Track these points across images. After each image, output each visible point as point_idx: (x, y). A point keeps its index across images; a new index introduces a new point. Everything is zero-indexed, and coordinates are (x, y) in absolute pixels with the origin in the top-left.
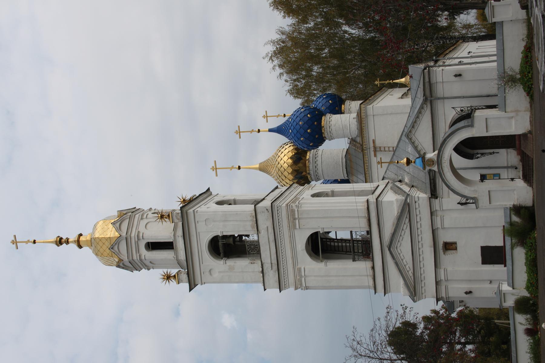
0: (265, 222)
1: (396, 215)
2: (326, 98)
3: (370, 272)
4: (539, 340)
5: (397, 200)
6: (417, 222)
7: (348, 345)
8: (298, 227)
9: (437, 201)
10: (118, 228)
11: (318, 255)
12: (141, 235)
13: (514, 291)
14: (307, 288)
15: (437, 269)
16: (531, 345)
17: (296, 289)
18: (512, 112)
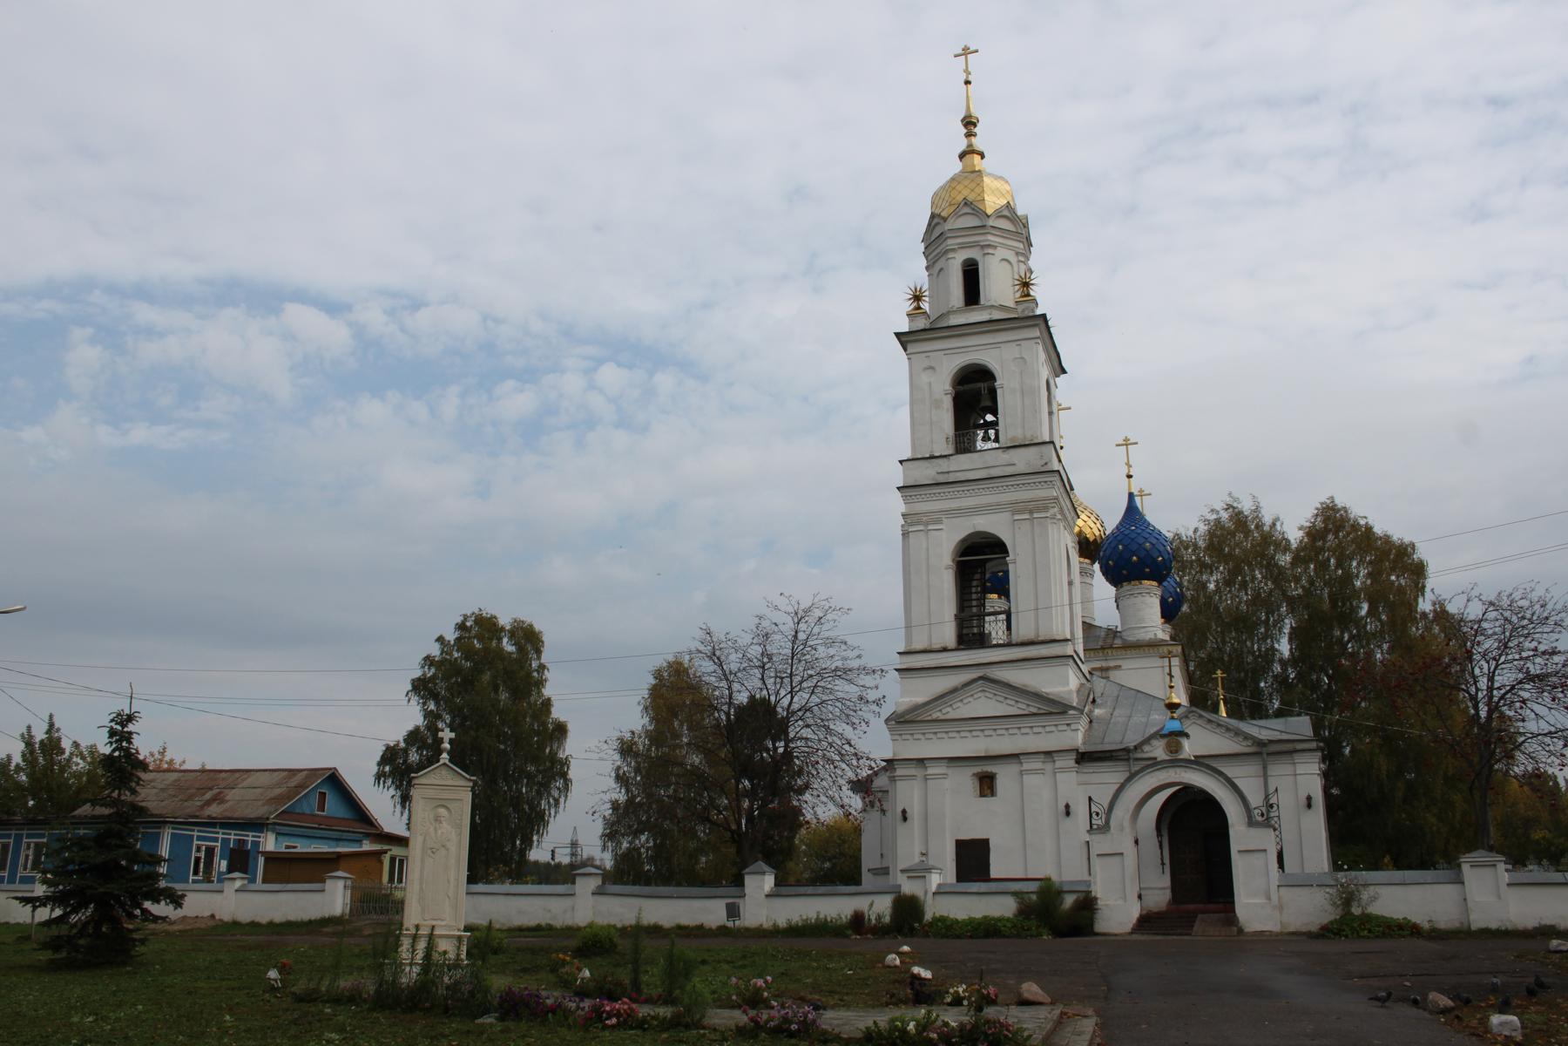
0: (1023, 460)
2: (1176, 591)
3: (937, 646)
4: (847, 937)
5: (1070, 692)
6: (1031, 727)
7: (816, 600)
8: (1016, 517)
9: (1072, 763)
11: (961, 556)
12: (990, 251)
13: (930, 895)
14: (905, 534)
15: (946, 761)
16: (831, 921)
17: (903, 515)
18: (1279, 898)
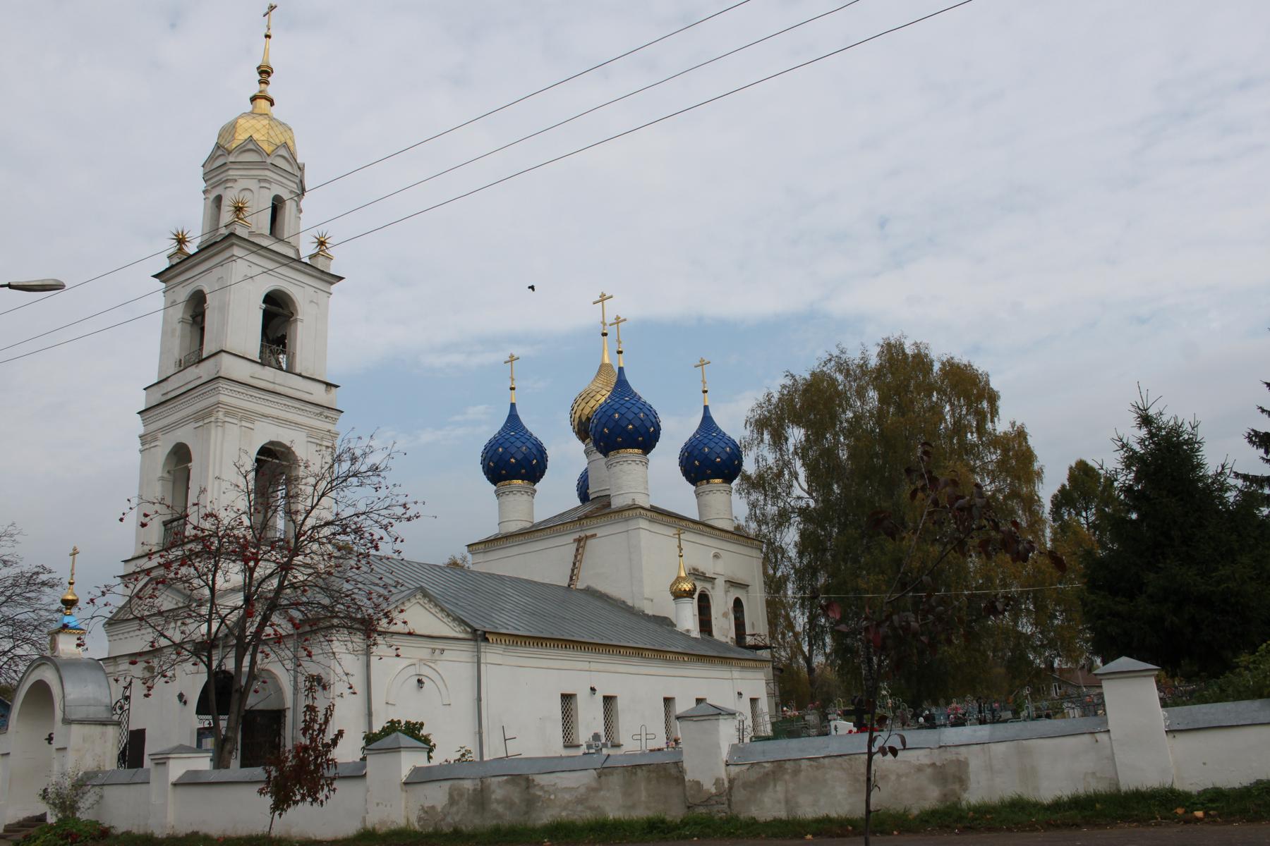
10: (245, 148)
17: (140, 437)
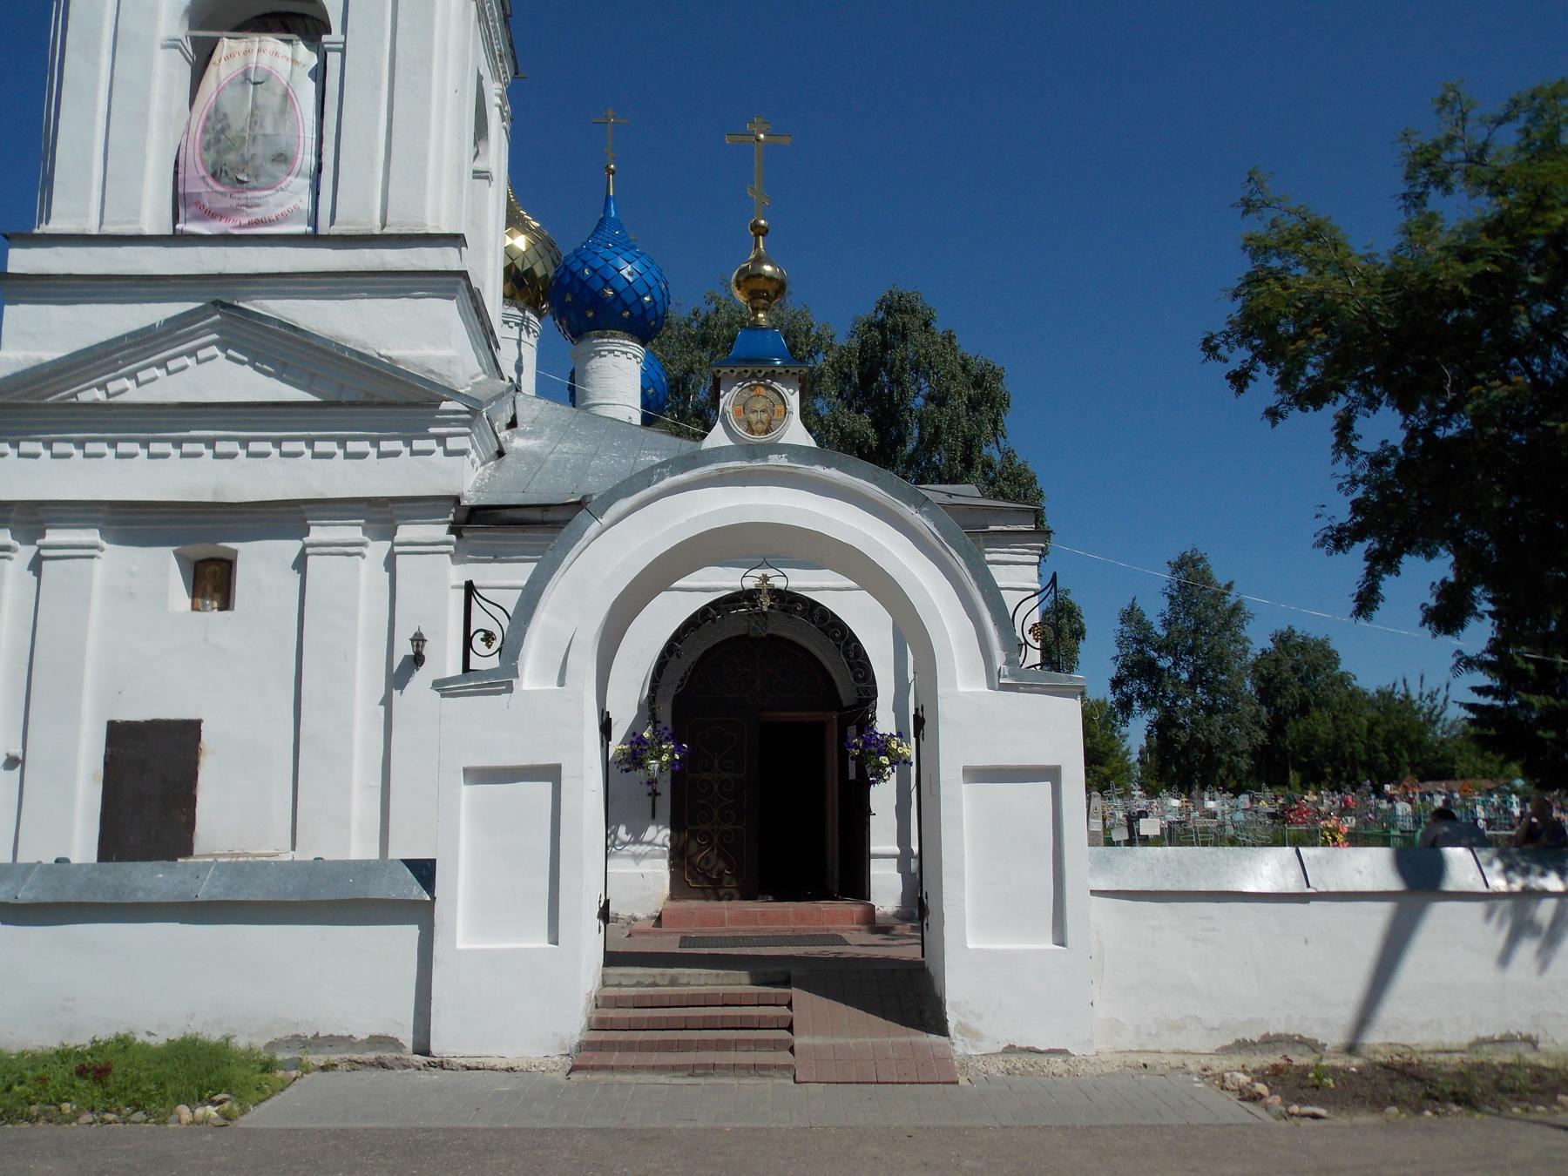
1: (383, 352)
9: (439, 531)
